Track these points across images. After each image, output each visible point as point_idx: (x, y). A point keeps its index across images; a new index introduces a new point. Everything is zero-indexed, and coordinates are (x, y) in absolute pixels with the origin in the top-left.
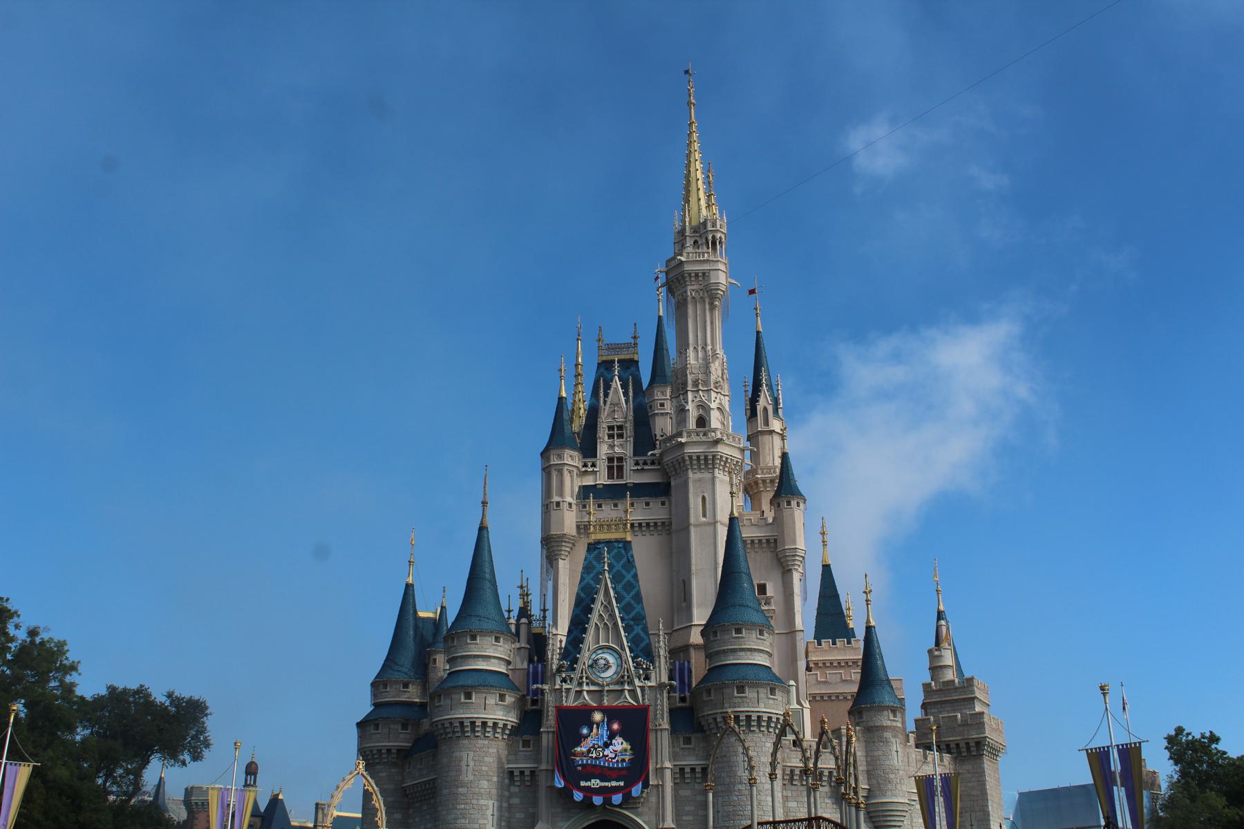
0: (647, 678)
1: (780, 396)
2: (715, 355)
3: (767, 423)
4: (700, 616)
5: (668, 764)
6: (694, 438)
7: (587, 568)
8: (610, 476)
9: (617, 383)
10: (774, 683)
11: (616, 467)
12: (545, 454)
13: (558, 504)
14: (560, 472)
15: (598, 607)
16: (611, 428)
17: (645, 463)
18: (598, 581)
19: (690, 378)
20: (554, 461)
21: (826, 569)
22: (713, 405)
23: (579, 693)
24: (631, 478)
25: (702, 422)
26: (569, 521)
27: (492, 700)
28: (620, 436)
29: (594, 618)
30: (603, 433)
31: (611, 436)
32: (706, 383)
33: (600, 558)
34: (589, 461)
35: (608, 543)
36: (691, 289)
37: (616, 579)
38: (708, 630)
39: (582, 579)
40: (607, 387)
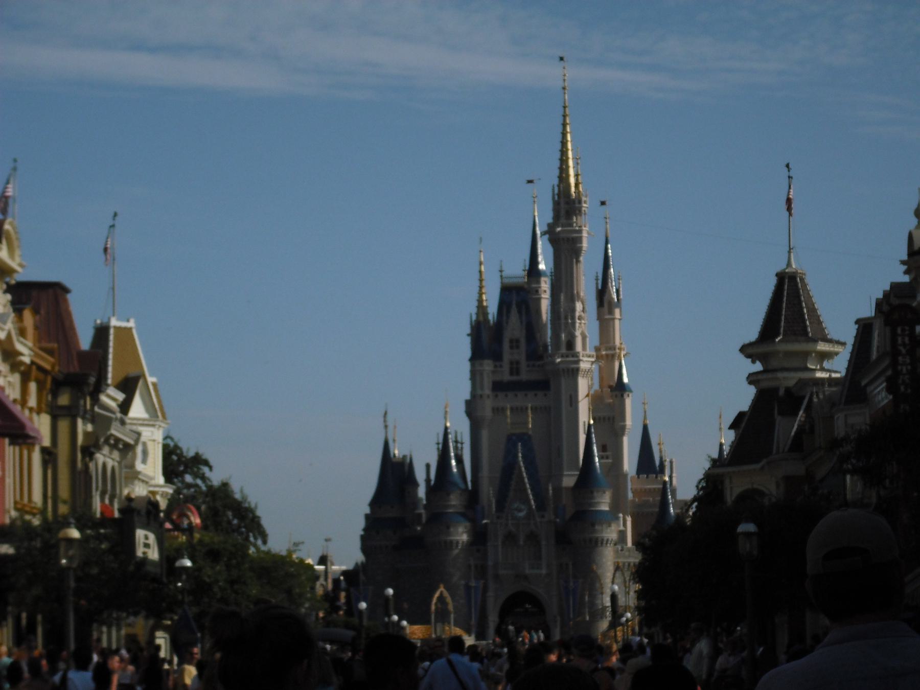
0: (543, 516)
1: (621, 289)
3: (611, 312)
8: (511, 374)
9: (514, 310)
11: (515, 368)
13: (481, 396)
14: (482, 374)
16: (511, 341)
17: (534, 366)
21: (645, 429)
24: (524, 376)
30: (506, 345)
31: (511, 347)
32: (573, 318)
33: (515, 446)
40: (508, 312)
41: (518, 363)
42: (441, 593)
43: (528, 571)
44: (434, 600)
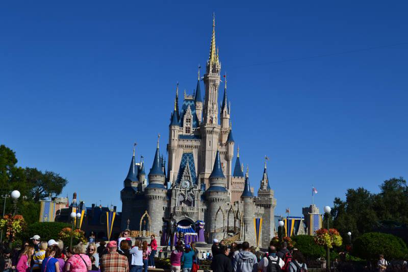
0: (196, 188)
2: (215, 103)
4: (208, 171)
5: (200, 208)
6: (209, 126)
7: (183, 160)
8: (186, 133)
10: (224, 190)
11: (188, 130)
12: (170, 126)
15: (185, 171)
16: (187, 119)
18: (185, 164)
19: (209, 109)
20: (173, 128)
22: (214, 117)
23: (180, 191)
25: (211, 121)
26: (175, 143)
27: (160, 191)
28: (190, 122)
29: (184, 173)
31: (187, 122)
33: (186, 158)
34: (181, 128)
35: (188, 154)
36: (211, 84)
37: (190, 163)
38: (211, 179)
39: (181, 163)
41: (189, 128)
42: (146, 215)
43: (188, 211)
44: (142, 218)
